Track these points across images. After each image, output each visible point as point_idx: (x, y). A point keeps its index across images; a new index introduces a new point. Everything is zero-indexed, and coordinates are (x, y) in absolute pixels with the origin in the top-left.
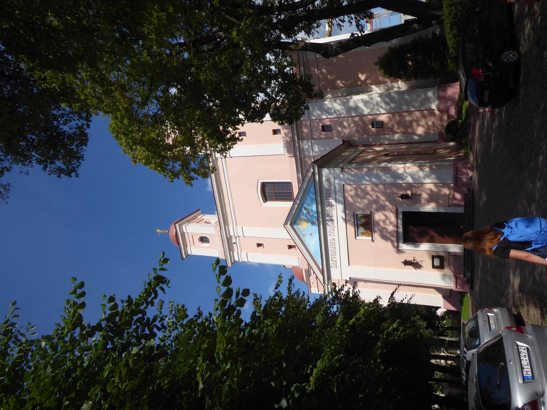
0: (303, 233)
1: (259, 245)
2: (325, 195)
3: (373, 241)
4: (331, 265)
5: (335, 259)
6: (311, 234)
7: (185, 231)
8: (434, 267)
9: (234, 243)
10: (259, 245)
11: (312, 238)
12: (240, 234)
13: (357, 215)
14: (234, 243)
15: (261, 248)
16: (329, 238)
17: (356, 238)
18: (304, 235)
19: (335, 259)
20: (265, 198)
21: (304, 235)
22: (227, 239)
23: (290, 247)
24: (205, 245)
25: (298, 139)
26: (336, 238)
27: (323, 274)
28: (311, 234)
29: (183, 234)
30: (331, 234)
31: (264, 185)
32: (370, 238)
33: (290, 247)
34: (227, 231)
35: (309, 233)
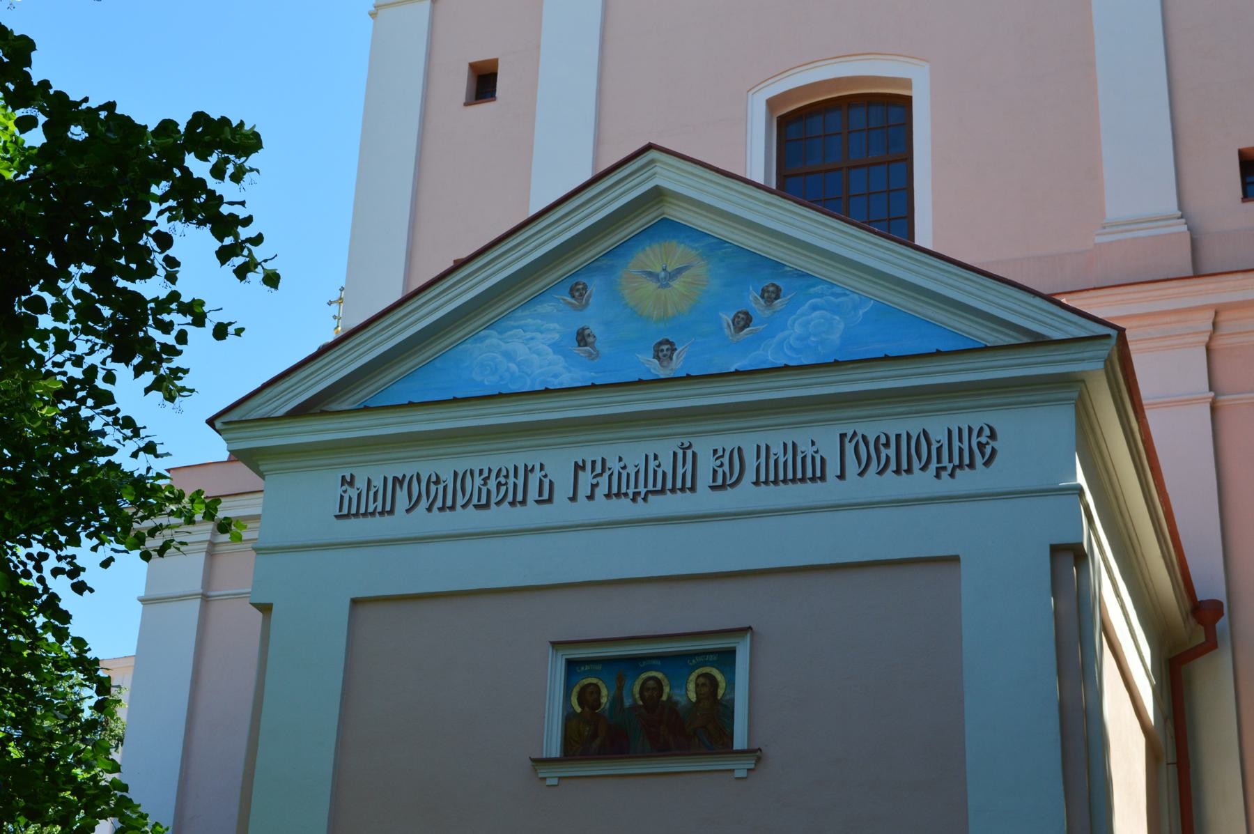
0: (595, 285)
1: (484, 83)
5: (402, 495)
6: (582, 338)
10: (484, 83)
11: (556, 347)
13: (726, 658)
15: (461, 83)
16: (557, 463)
17: (555, 644)
18: (578, 292)
21: (578, 292)
26: (561, 511)
27: (301, 412)
28: (582, 338)
30: (586, 478)
35: (595, 328)
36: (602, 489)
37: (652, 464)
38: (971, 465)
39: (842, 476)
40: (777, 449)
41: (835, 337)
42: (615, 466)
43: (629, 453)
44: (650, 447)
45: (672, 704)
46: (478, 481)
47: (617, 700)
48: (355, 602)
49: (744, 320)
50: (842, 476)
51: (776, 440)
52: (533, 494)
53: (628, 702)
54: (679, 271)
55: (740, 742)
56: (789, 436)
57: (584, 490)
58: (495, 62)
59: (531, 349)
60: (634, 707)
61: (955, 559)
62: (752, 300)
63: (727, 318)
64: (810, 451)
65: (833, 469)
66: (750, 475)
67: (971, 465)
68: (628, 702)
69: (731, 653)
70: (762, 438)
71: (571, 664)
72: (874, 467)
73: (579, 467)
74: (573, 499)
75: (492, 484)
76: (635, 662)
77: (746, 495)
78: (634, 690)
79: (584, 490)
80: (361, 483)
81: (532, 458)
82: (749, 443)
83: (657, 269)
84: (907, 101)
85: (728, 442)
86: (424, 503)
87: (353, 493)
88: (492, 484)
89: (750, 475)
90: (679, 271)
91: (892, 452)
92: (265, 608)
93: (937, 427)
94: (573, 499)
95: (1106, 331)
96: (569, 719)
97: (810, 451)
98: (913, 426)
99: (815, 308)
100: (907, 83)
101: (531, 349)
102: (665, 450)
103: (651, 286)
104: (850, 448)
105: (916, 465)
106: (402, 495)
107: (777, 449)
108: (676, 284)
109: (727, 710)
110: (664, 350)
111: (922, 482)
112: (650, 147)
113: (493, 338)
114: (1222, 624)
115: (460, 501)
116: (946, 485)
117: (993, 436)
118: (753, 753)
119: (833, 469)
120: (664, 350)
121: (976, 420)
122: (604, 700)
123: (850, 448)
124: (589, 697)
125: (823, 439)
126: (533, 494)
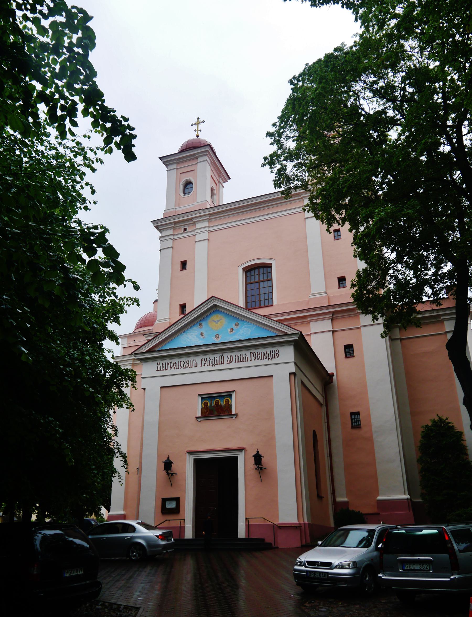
1: (184, 265)
2: (256, 351)
3: (197, 418)
4: (161, 362)
5: (169, 366)
6: (202, 334)
7: (200, 160)
8: (164, 501)
9: (185, 230)
10: (184, 265)
11: (197, 336)
12: (198, 238)
14: (185, 230)
15: (179, 266)
16: (198, 359)
17: (199, 395)
19: (169, 368)
20: (248, 270)
22: (191, 219)
23: (183, 307)
24: (181, 188)
25: (333, 313)
26: (199, 369)
27: (148, 352)
28: (202, 334)
29: (195, 157)
30: (203, 362)
31: (269, 266)
32: (200, 415)
33: (183, 307)
34: (201, 219)
35: (204, 332)
36: (206, 364)
37: (216, 359)
38: (275, 358)
39: (251, 360)
40: (239, 355)
41: (249, 333)
42: (209, 359)
43: (211, 357)
44: (215, 356)
45: (221, 405)
46: (183, 363)
47: (211, 405)
48: (161, 387)
49: (232, 330)
50: (251, 360)
51: (239, 354)
52: (194, 365)
53: (213, 405)
54: (220, 320)
55: (233, 413)
56: (241, 353)
57: (203, 364)
58: (186, 261)
59: (192, 338)
60: (214, 406)
61: (272, 376)
62: (233, 326)
63: (229, 330)
64: (245, 356)
65: (249, 359)
66: (234, 361)
67: (275, 358)
68: (213, 405)
69: (232, 395)
70: (236, 353)
71: (202, 398)
72: (257, 358)
73: (202, 360)
74: (201, 366)
75: (186, 363)
76: (214, 397)
77: (233, 365)
78: (214, 404)
79: (203, 364)
80: (161, 364)
81: (193, 358)
82: (233, 354)
83: (215, 320)
84: (271, 267)
85: (230, 354)
86: (173, 368)
87: (159, 366)
88: (186, 363)
89: (234, 361)
90: (220, 320)
91: (260, 355)
92: (144, 389)
93: (268, 350)
94: (201, 366)
95: (297, 332)
96: (202, 409)
97: (245, 356)
98: (263, 350)
99: (245, 327)
100: (271, 264)
101: (192, 338)
102: (218, 356)
103: (214, 323)
104: (252, 355)
105: (265, 358)
106: (169, 366)
107: (239, 355)
108: (219, 323)
109: (231, 406)
110: (217, 336)
111: (266, 361)
112: (213, 297)
113: (185, 335)
114: (335, 377)
115: (180, 367)
116: (270, 362)
117: (278, 352)
118: (236, 415)
119: (249, 359)
120: (217, 336)
121: (275, 349)
122: (209, 405)
123: (252, 355)
124: (206, 404)
125: (247, 354)
126: (194, 365)
